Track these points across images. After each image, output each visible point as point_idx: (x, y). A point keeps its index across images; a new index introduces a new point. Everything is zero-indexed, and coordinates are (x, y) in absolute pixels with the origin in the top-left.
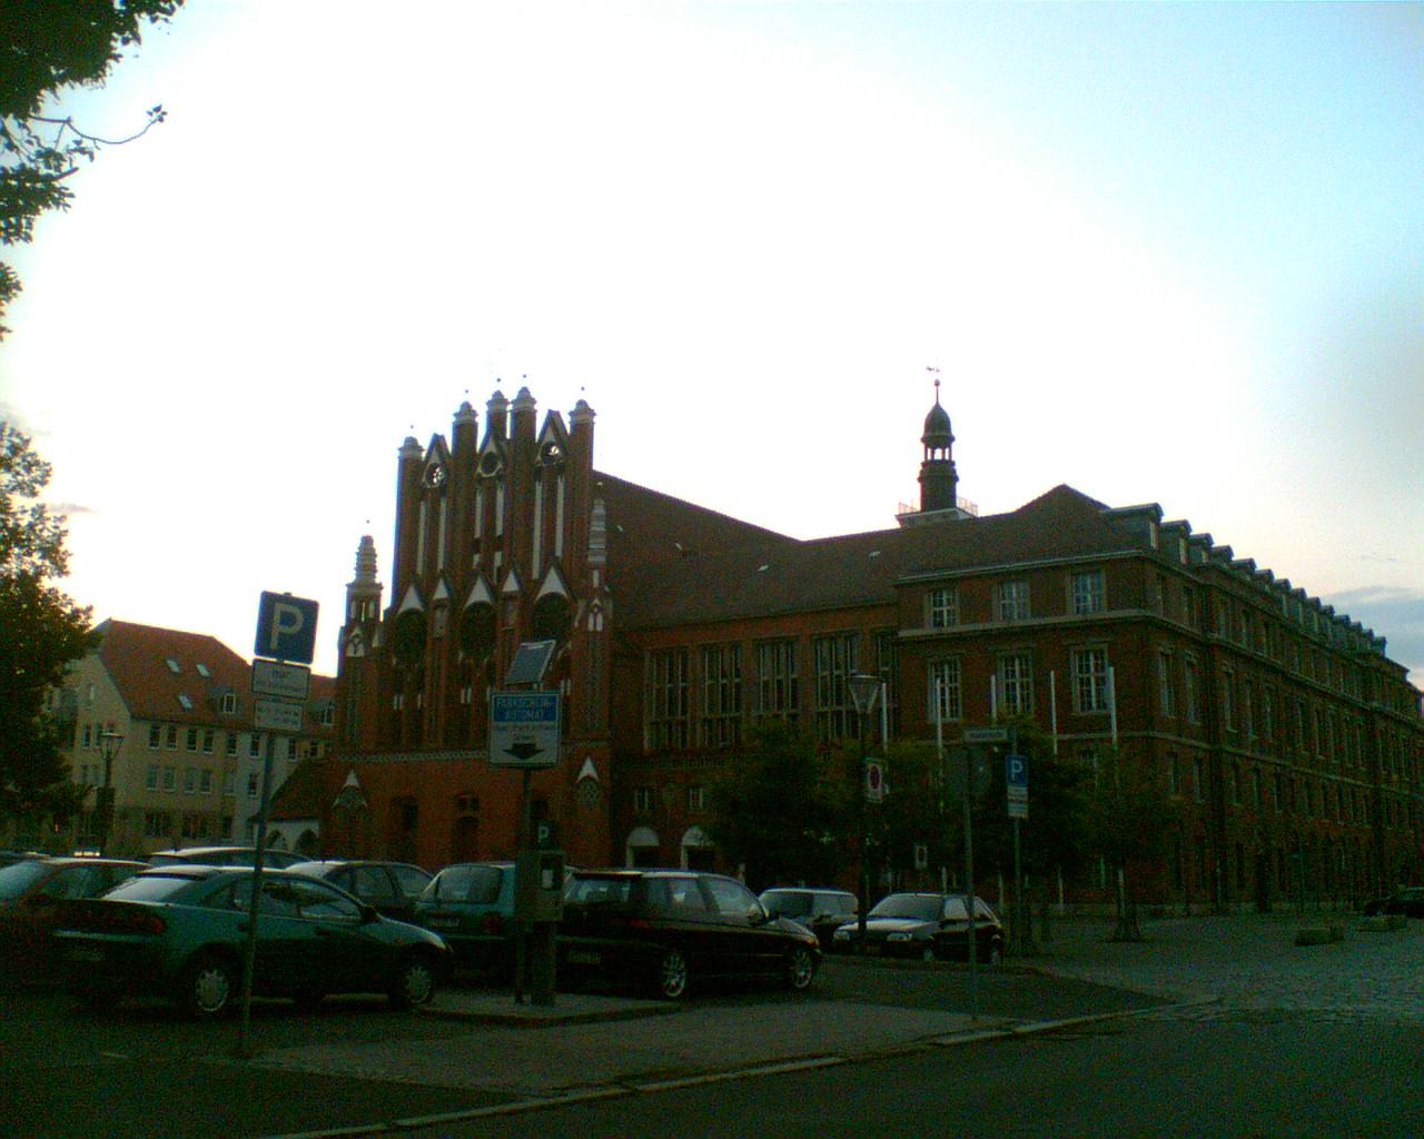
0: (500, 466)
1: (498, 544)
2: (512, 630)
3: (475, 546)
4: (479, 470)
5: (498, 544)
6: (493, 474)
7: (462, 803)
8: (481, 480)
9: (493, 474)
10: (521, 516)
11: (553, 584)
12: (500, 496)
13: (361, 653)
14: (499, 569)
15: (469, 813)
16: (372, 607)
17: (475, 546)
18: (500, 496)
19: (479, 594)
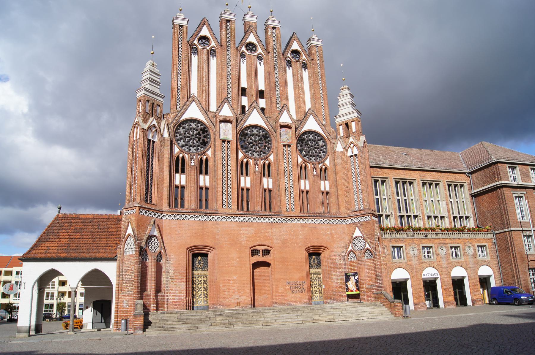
0: (260, 51)
1: (261, 94)
2: (289, 146)
3: (244, 92)
4: (244, 49)
5: (261, 94)
6: (256, 54)
7: (254, 252)
8: (243, 55)
9: (256, 54)
10: (275, 83)
11: (311, 125)
12: (261, 68)
13: (156, 140)
14: (263, 110)
15: (260, 258)
16: (159, 109)
17: (244, 92)
18: (261, 68)
19: (255, 119)
